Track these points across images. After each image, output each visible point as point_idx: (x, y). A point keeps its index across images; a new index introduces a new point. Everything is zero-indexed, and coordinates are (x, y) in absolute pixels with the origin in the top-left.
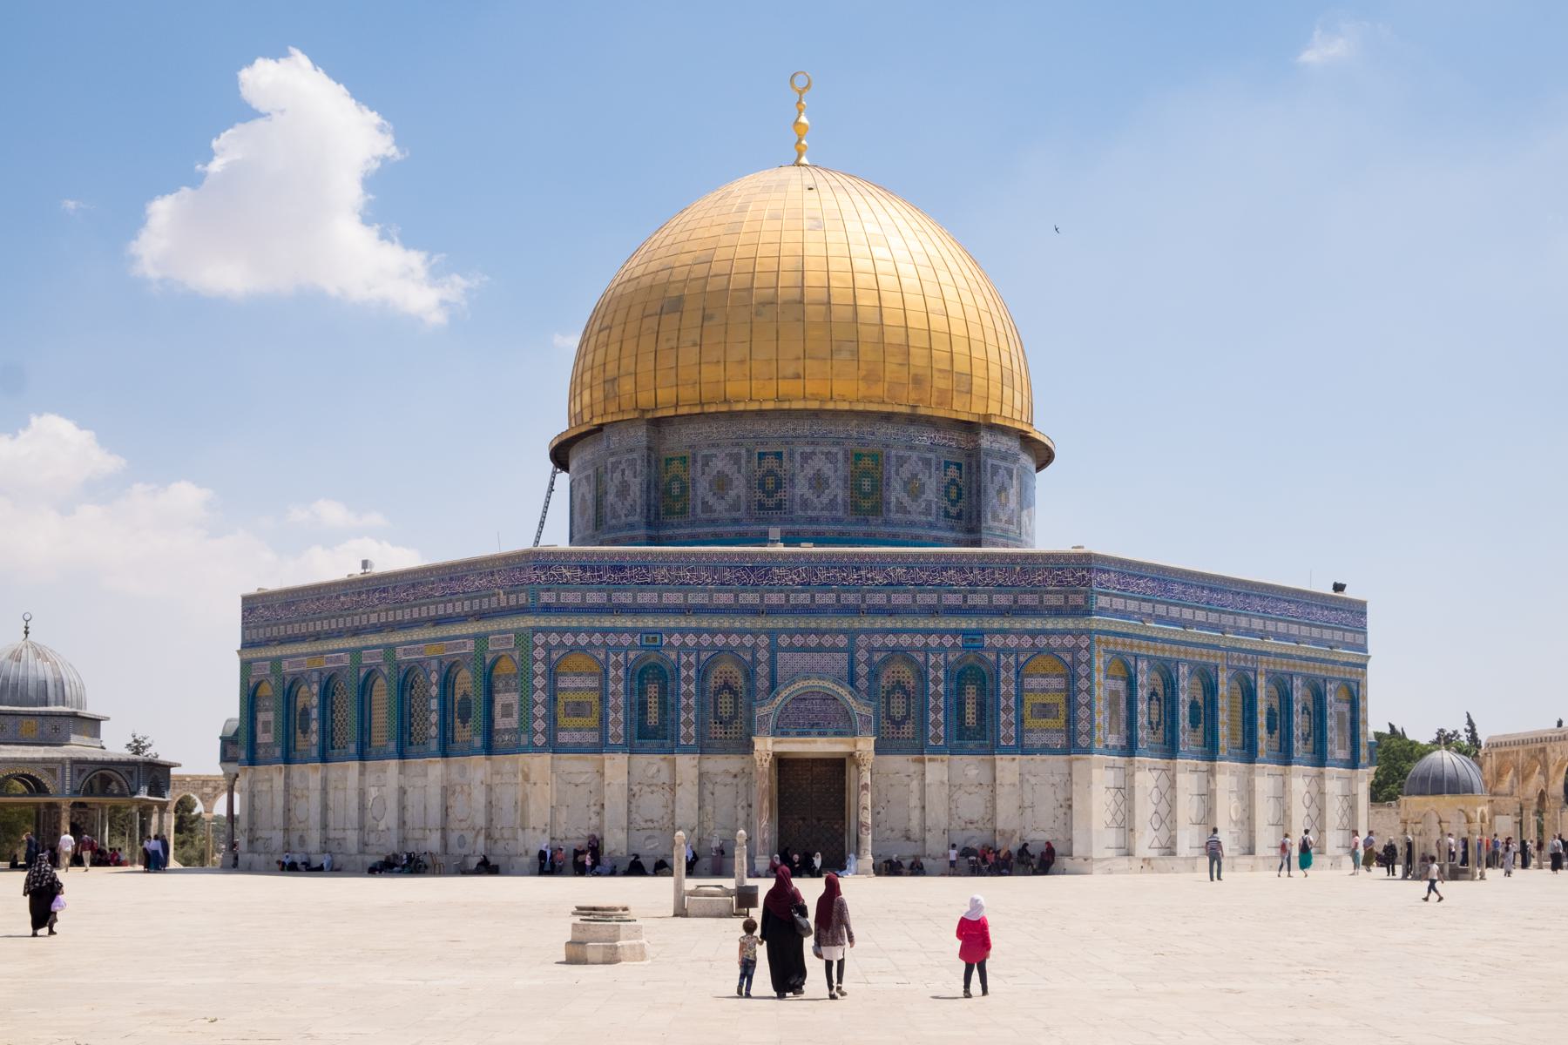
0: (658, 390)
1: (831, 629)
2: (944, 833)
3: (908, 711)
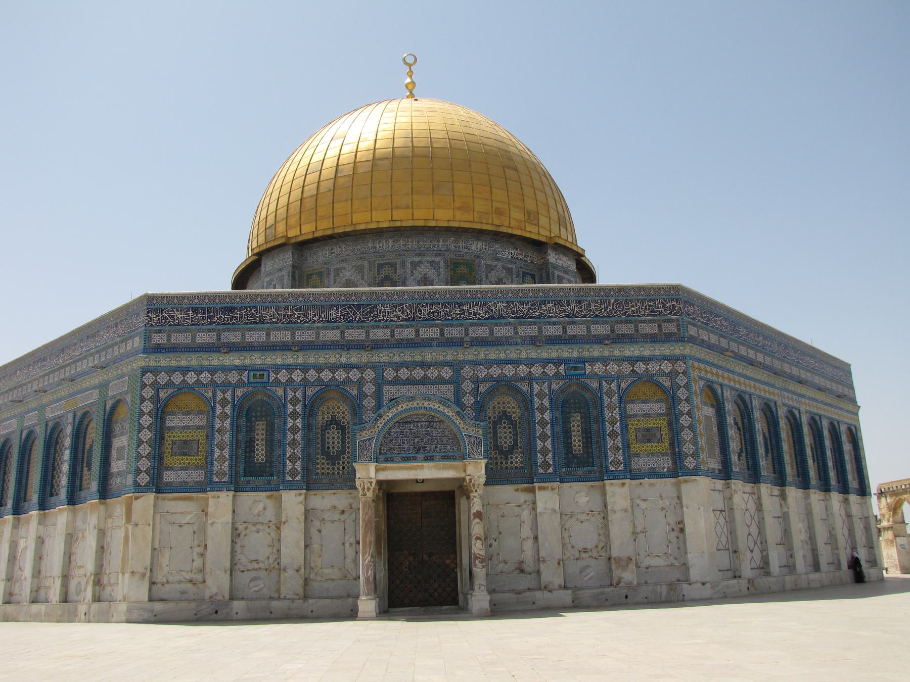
0: (302, 226)
1: (436, 362)
2: (559, 563)
3: (516, 441)
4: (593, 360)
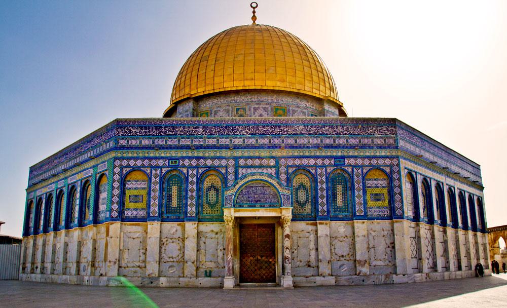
1: (266, 156)
2: (329, 263)
4: (350, 157)
